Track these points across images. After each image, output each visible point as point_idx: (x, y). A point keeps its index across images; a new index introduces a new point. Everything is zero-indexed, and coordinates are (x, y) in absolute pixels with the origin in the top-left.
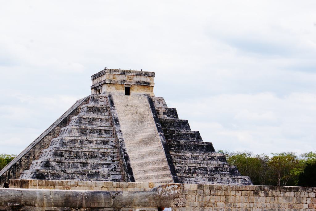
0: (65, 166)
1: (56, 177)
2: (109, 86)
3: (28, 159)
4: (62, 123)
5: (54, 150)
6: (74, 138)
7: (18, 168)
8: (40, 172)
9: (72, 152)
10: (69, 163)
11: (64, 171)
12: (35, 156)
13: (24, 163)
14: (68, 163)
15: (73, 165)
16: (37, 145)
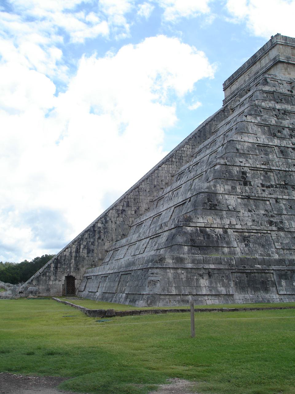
0: (266, 210)
1: (255, 243)
2: (286, 69)
3: (124, 216)
4: (196, 137)
5: (218, 167)
6: (261, 141)
7: (99, 238)
8: (199, 225)
9: (272, 174)
10: (277, 202)
11: (276, 224)
12: (138, 209)
13: (114, 226)
14: (273, 201)
15: (291, 208)
16: (143, 184)
